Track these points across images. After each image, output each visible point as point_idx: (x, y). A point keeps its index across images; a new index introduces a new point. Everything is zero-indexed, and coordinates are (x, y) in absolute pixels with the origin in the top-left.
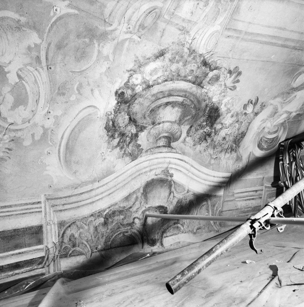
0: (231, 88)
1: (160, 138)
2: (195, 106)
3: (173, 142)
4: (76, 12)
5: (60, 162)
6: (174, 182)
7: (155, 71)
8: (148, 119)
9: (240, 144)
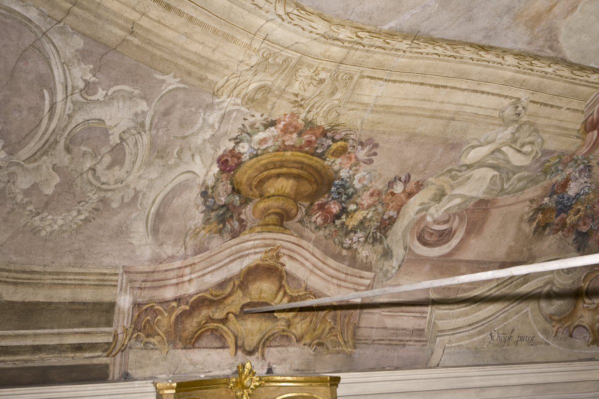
0: (366, 161)
1: (269, 214)
2: (316, 179)
3: (287, 221)
4: (186, 86)
5: (147, 230)
6: (287, 273)
7: (264, 140)
8: (255, 190)
9: (388, 233)
